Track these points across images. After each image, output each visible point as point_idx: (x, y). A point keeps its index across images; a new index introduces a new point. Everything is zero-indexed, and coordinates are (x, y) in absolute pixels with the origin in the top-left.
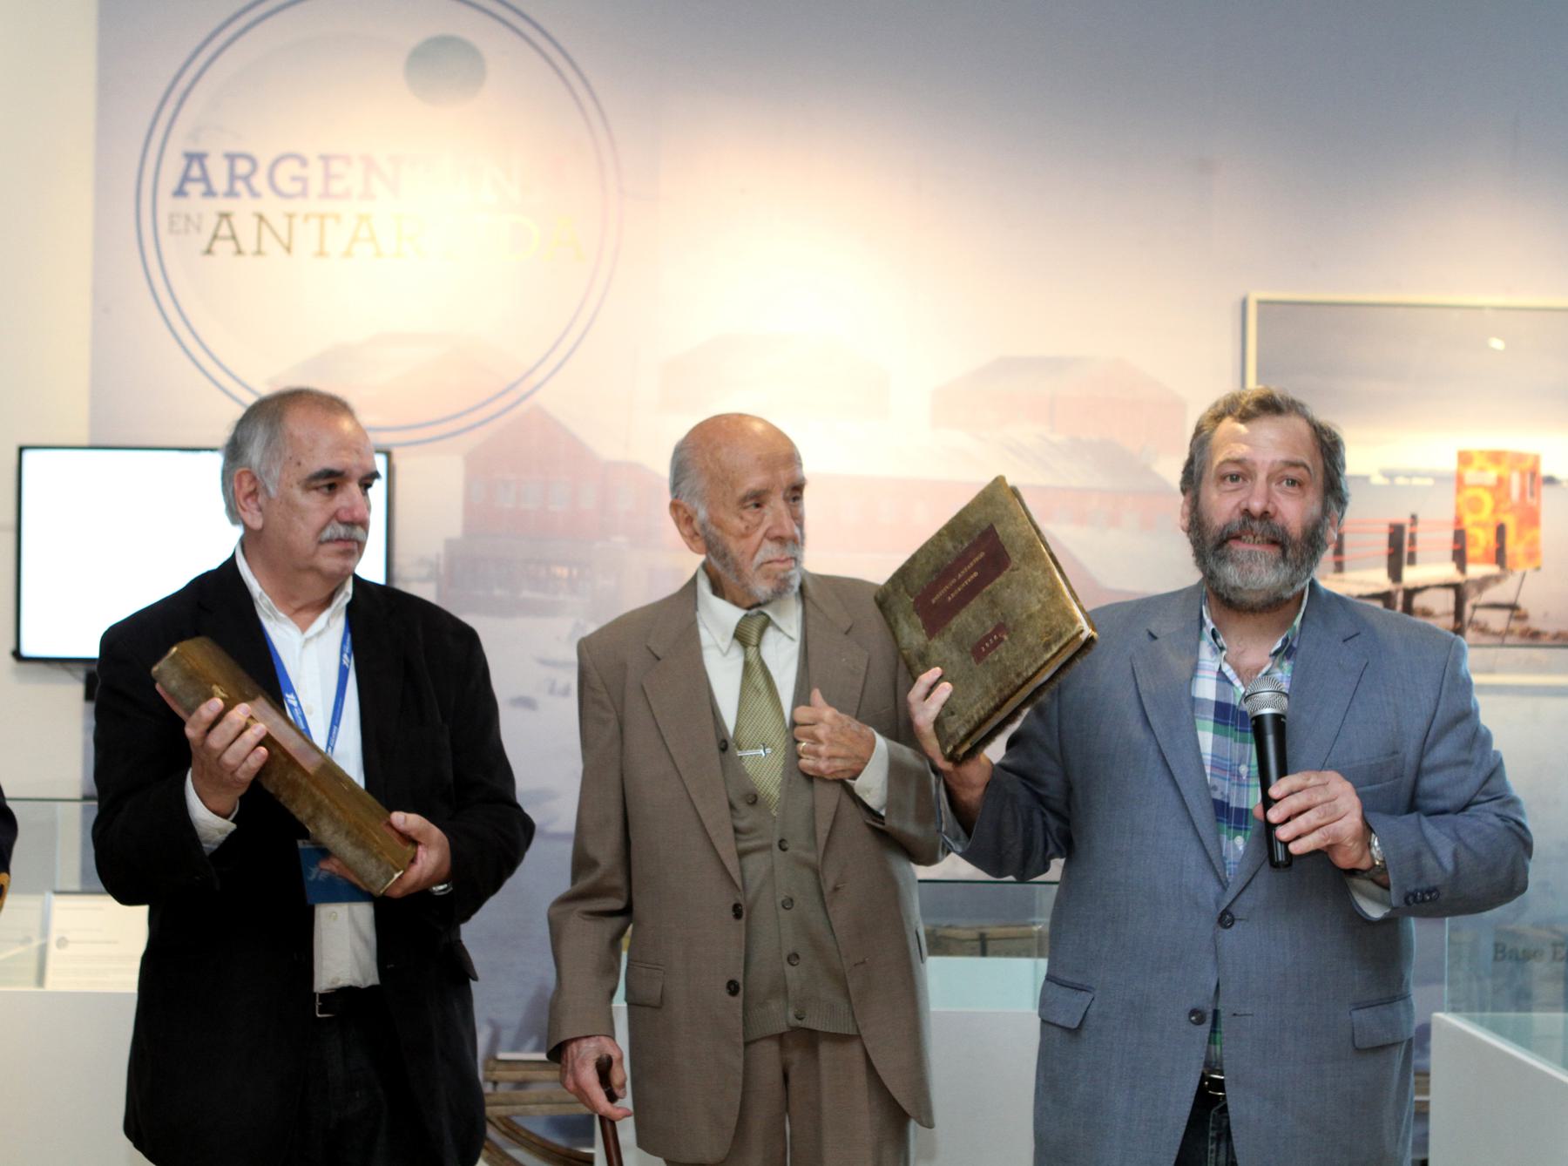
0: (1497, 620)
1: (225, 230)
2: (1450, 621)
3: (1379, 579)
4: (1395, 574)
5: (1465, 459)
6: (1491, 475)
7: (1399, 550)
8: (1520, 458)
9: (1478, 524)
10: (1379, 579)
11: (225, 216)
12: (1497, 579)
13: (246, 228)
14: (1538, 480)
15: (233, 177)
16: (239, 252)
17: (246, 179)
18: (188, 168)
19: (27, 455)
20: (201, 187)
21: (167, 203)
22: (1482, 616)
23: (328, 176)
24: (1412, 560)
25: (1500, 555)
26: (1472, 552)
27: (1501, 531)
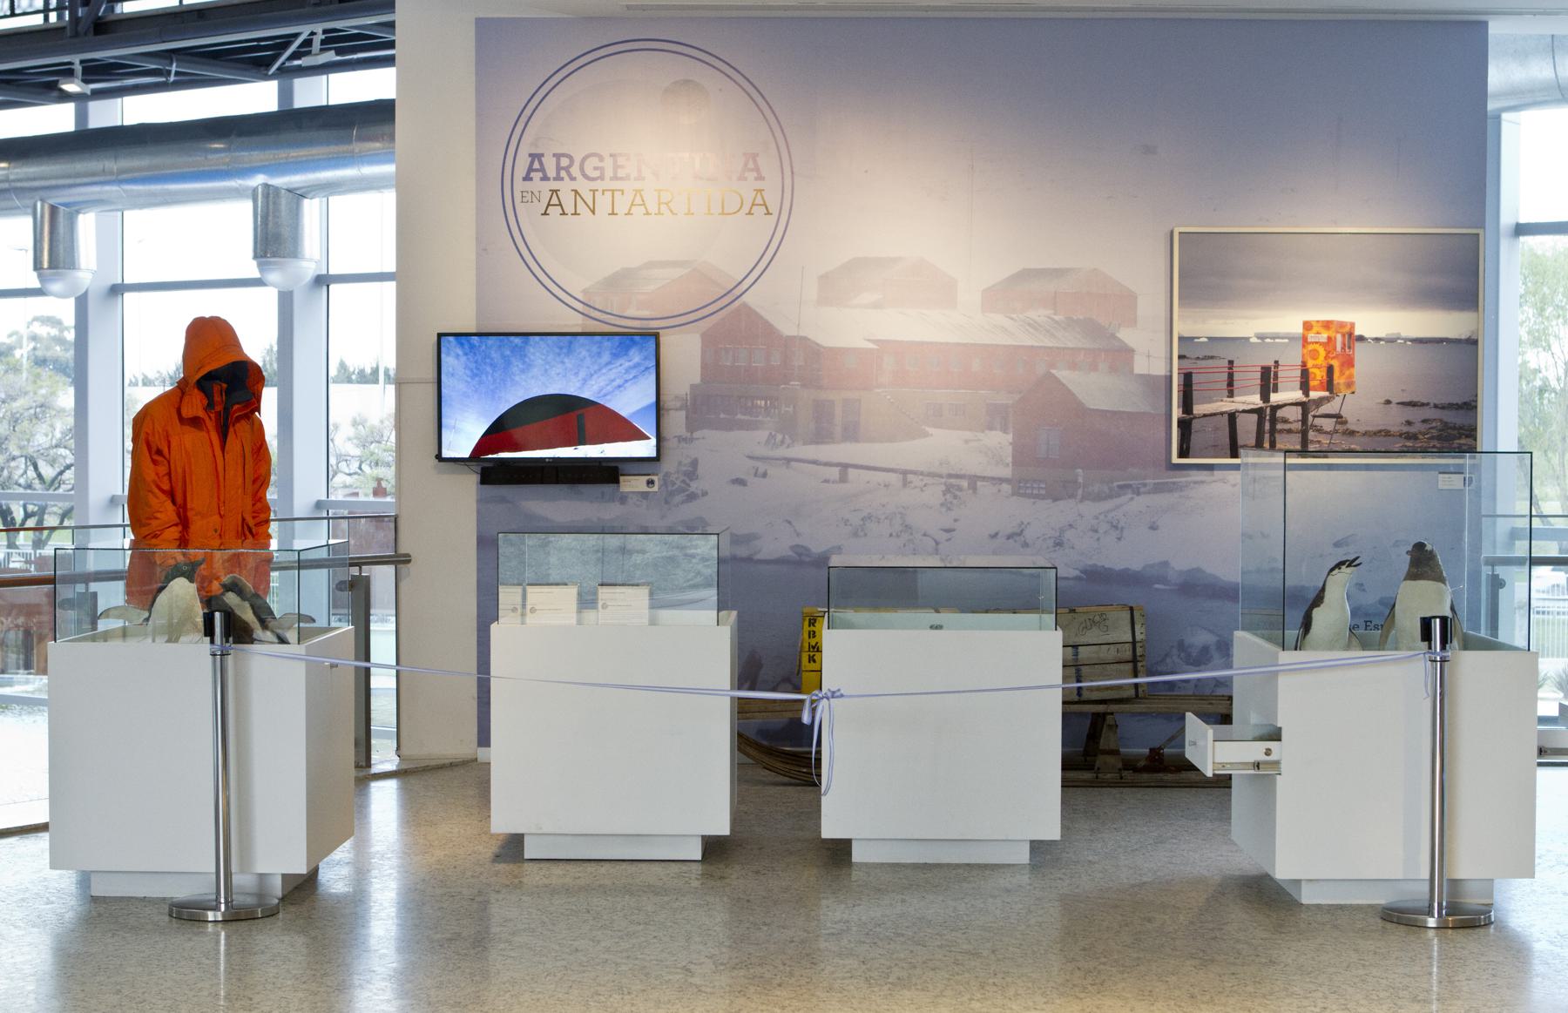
0: (1328, 424)
1: (555, 201)
2: (1298, 426)
3: (1255, 400)
4: (1265, 397)
5: (1308, 326)
6: (1324, 337)
7: (1268, 381)
8: (1342, 325)
9: (1315, 366)
10: (1255, 400)
12: (1328, 399)
13: (568, 200)
14: (1353, 339)
15: (559, 168)
17: (567, 169)
18: (532, 163)
21: (520, 185)
22: (1318, 421)
23: (616, 167)
24: (1276, 390)
25: (1329, 385)
26: (1312, 383)
27: (1330, 369)
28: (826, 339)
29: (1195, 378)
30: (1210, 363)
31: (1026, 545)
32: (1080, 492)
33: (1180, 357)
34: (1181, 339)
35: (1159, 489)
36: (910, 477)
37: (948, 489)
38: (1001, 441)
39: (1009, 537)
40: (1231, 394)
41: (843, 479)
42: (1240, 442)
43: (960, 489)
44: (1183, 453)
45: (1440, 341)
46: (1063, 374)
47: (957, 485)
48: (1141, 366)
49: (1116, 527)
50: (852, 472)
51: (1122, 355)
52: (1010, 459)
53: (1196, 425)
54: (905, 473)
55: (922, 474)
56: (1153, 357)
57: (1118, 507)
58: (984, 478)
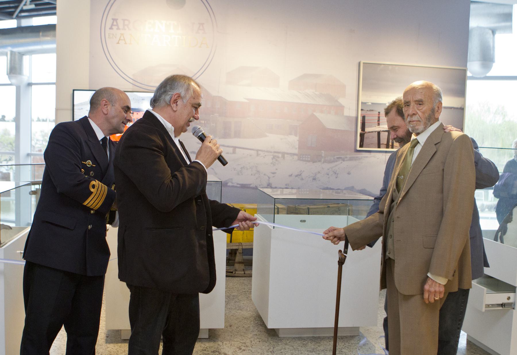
11: (122, 34)
16: (126, 43)
18: (113, 23)
19: (75, 92)
20: (116, 27)
21: (108, 31)
28: (229, 98)
29: (366, 118)
30: (371, 112)
31: (302, 179)
32: (323, 160)
33: (362, 110)
34: (362, 103)
35: (351, 159)
36: (259, 152)
37: (274, 157)
38: (294, 139)
39: (296, 176)
40: (379, 124)
41: (234, 152)
42: (381, 142)
43: (278, 157)
44: (361, 146)
45: (451, 108)
46: (318, 115)
47: (277, 156)
48: (346, 113)
49: (335, 173)
50: (237, 150)
51: (340, 108)
52: (297, 147)
53: (366, 135)
54: (258, 150)
55: (264, 151)
56: (351, 110)
57: (336, 166)
58: (287, 154)
